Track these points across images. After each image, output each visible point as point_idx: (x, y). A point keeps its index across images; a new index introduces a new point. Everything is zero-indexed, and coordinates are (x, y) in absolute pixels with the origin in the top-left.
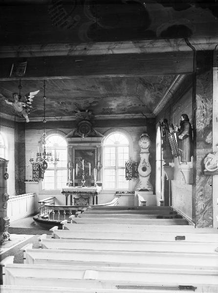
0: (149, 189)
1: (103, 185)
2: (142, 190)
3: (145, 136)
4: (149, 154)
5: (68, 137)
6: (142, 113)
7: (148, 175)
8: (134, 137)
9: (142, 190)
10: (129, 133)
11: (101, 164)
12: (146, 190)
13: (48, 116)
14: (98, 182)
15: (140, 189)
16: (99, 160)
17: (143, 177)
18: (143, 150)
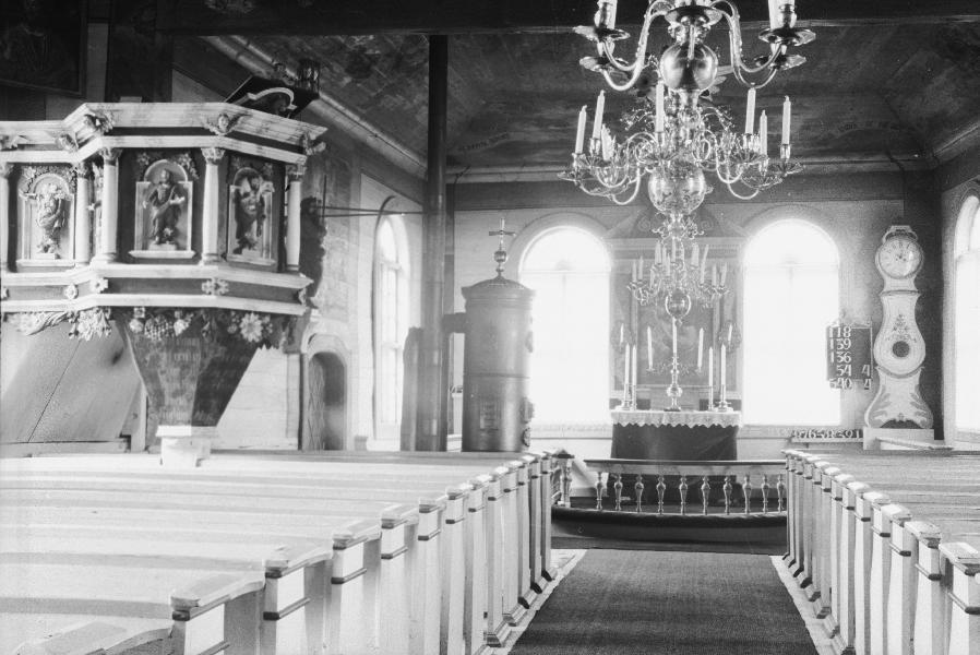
0: (918, 420)
1: (745, 405)
2: (892, 424)
3: (900, 234)
4: (915, 297)
5: (616, 237)
6: (888, 154)
7: (915, 372)
8: (856, 238)
9: (892, 424)
10: (829, 222)
11: (737, 334)
12: (910, 424)
13: (542, 164)
14: (733, 397)
15: (884, 419)
16: (728, 316)
17: (900, 377)
18: (890, 284)
